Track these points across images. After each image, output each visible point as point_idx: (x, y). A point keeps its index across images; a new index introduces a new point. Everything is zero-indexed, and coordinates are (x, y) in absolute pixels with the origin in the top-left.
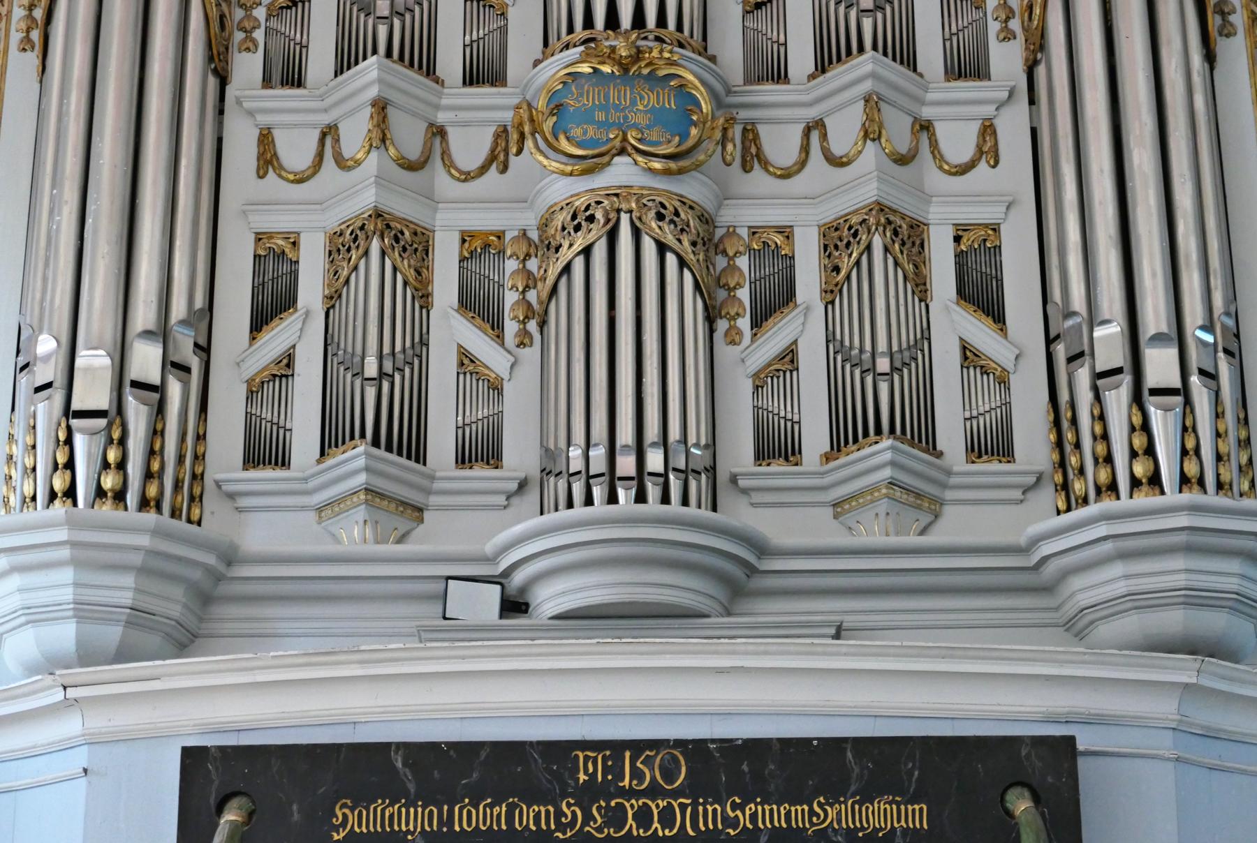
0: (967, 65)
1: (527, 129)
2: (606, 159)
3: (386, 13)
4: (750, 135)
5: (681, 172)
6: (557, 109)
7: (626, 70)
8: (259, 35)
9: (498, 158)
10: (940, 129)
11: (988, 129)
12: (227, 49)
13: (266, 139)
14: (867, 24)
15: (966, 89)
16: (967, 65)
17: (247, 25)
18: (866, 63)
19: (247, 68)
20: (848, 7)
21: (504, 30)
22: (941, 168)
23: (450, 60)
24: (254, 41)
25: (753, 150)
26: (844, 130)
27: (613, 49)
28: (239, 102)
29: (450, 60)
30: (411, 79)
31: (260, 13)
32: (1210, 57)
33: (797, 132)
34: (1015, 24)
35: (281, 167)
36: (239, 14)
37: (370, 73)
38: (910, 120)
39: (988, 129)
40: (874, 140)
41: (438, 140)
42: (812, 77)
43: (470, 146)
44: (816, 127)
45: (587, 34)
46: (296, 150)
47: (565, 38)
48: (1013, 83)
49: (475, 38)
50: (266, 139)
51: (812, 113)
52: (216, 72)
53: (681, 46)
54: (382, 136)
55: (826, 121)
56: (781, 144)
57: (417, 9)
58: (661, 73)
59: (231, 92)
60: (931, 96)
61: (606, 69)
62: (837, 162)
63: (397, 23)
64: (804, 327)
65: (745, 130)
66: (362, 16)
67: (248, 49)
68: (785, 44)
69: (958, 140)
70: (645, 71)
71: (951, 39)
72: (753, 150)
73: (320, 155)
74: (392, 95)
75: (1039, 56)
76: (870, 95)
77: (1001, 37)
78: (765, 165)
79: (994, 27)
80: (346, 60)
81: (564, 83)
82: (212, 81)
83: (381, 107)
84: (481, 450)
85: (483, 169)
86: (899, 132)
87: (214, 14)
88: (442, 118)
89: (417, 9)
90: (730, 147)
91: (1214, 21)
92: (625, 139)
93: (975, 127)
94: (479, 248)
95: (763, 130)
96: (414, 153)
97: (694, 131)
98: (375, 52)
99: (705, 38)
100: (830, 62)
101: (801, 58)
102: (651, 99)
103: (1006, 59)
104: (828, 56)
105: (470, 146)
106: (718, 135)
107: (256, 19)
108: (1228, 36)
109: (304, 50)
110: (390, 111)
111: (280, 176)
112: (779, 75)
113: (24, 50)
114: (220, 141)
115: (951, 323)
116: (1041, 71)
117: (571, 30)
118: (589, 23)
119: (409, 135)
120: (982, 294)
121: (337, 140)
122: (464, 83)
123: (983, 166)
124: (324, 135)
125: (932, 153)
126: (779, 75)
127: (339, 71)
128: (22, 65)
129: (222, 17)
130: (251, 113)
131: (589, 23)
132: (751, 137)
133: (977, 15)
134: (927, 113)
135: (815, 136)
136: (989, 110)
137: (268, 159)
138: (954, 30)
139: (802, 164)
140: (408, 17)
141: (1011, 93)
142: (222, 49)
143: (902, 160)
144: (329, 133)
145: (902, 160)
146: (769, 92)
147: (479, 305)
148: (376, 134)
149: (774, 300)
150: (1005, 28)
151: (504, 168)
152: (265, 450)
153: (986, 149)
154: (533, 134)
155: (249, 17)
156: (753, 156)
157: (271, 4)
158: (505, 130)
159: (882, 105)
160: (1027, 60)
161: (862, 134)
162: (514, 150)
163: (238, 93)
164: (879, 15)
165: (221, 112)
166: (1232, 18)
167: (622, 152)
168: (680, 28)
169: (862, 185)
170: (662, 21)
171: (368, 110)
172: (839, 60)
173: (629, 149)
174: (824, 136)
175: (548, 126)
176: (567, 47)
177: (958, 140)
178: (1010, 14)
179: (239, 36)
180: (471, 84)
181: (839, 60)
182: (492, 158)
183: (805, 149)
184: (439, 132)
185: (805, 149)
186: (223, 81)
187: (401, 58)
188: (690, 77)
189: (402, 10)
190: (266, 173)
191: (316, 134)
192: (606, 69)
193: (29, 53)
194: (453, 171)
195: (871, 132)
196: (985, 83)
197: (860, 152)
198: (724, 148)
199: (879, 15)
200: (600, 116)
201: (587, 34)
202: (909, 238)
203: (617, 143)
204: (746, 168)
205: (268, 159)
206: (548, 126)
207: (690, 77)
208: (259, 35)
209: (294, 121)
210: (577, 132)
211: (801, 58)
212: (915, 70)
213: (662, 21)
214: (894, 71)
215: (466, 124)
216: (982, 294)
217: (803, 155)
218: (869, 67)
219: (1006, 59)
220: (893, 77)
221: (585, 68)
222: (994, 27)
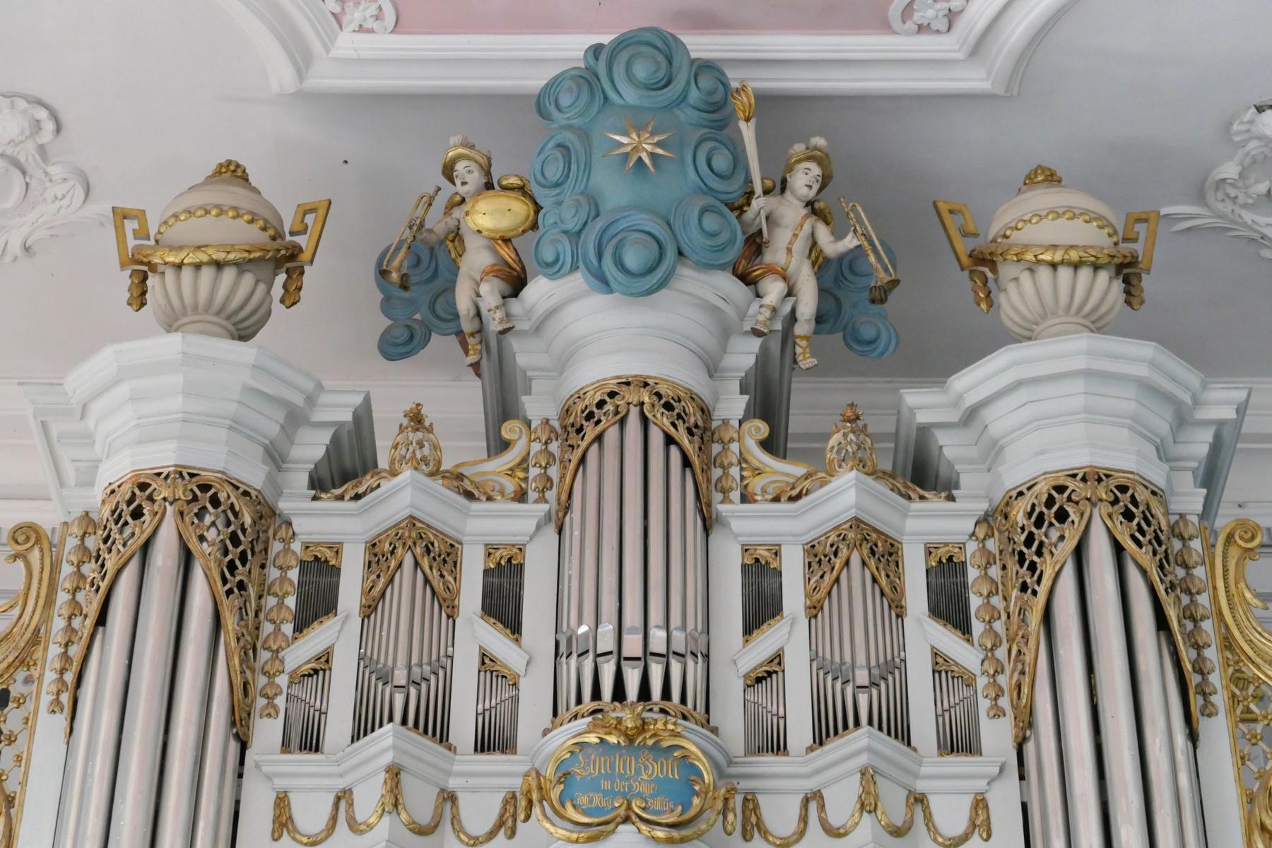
0: (958, 741)
1: (535, 796)
2: (611, 827)
3: (403, 682)
4: (751, 805)
5: (683, 840)
6: (565, 777)
7: (631, 740)
8: (280, 701)
9: (506, 823)
10: (935, 803)
11: (980, 804)
12: (249, 714)
13: (282, 802)
14: (863, 699)
15: (959, 764)
16: (958, 741)
17: (270, 692)
18: (862, 739)
19: (267, 732)
20: (846, 682)
21: (515, 700)
22: (935, 840)
23: (463, 727)
24: (275, 707)
25: (754, 820)
26: (842, 801)
27: (619, 720)
28: (258, 766)
29: (463, 727)
30: (425, 746)
31: (282, 681)
32: (1193, 737)
33: (795, 803)
34: (1004, 702)
35: (296, 830)
36: (262, 681)
37: (387, 740)
38: (904, 793)
39: (980, 804)
40: (870, 812)
41: (448, 805)
42: (810, 749)
43: (479, 812)
44: (814, 798)
45: (595, 705)
46: (311, 813)
47: (574, 708)
48: (1003, 759)
49: (487, 706)
50: (282, 802)
51: (810, 785)
52: (237, 736)
53: (685, 717)
54: (395, 800)
55: (824, 793)
57: (433, 678)
58: (665, 744)
59: (249, 754)
60: (924, 770)
61: (613, 739)
62: (834, 833)
63: (413, 691)
65: (745, 799)
66: (380, 684)
67: (269, 715)
68: (785, 717)
70: (650, 742)
71: (943, 716)
72: (754, 820)
73: (334, 819)
74: (405, 761)
75: (1028, 733)
76: (866, 769)
77: (992, 714)
78: (765, 834)
79: (984, 704)
80: (363, 727)
81: (572, 752)
82: (234, 746)
83: (395, 773)
85: (492, 835)
86: (894, 805)
87: (238, 682)
88: (453, 784)
89: (433, 678)
90: (731, 817)
91: (1196, 702)
92: (629, 808)
93: (966, 802)
95: (761, 799)
96: (425, 818)
97: (696, 801)
98: (391, 720)
99: (707, 711)
100: (828, 735)
101: (800, 729)
102: (655, 769)
103: (996, 735)
104: (824, 731)
106: (719, 805)
107: (278, 686)
108: (1209, 716)
109: (323, 717)
110: (403, 776)
111: (294, 839)
112: (777, 746)
113: (53, 712)
114: (238, 803)
116: (1030, 748)
117: (579, 701)
118: (596, 695)
119: (421, 802)
121: (351, 804)
122: (476, 750)
123: (976, 838)
124: (338, 799)
125: (927, 825)
126: (777, 746)
127: (355, 738)
128: (50, 726)
129: (246, 684)
130: (269, 777)
131: (596, 695)
132: (751, 806)
133: (967, 692)
134: (921, 786)
135: (813, 806)
136: (981, 785)
137: (283, 822)
138: (946, 706)
139: (801, 834)
140: (424, 685)
141: (1002, 769)
142: (244, 715)
143: (898, 832)
144: (343, 797)
145: (898, 832)
146: (769, 763)
148: (389, 800)
150: (995, 705)
151: (512, 834)
153: (978, 822)
154: (540, 802)
155: (271, 683)
157: (295, 671)
158: (514, 797)
159: (877, 778)
160: (1016, 737)
161: (858, 806)
162: (522, 816)
163: (257, 758)
164: (874, 692)
165: (240, 776)
166: (1213, 699)
167: (626, 820)
168: (683, 700)
170: (666, 694)
171: (382, 776)
172: (836, 733)
173: (633, 817)
174: (822, 807)
175: (555, 794)
176: (575, 717)
178: (999, 693)
179: (261, 702)
180: (482, 751)
181: (836, 733)
182: (500, 824)
183: (804, 819)
184: (450, 797)
185: (804, 819)
186: (244, 747)
187: (416, 725)
188: (693, 748)
189: (418, 679)
190: (281, 836)
191: (331, 798)
192: (613, 739)
193: (58, 715)
194: (462, 836)
195: (867, 805)
196: (977, 759)
197: (857, 824)
198: (725, 817)
199: (874, 692)
200: (606, 785)
201: (595, 705)
203: (622, 812)
204: (746, 836)
205: (283, 822)
206: (555, 794)
207: (693, 748)
208: (280, 701)
209: (310, 784)
210: (583, 800)
211: (800, 729)
212: (909, 744)
213: (666, 694)
214: (888, 746)
215: (475, 790)
217: (802, 826)
218: (865, 742)
219: (996, 735)
220: (887, 751)
221: (592, 738)
222: (984, 704)
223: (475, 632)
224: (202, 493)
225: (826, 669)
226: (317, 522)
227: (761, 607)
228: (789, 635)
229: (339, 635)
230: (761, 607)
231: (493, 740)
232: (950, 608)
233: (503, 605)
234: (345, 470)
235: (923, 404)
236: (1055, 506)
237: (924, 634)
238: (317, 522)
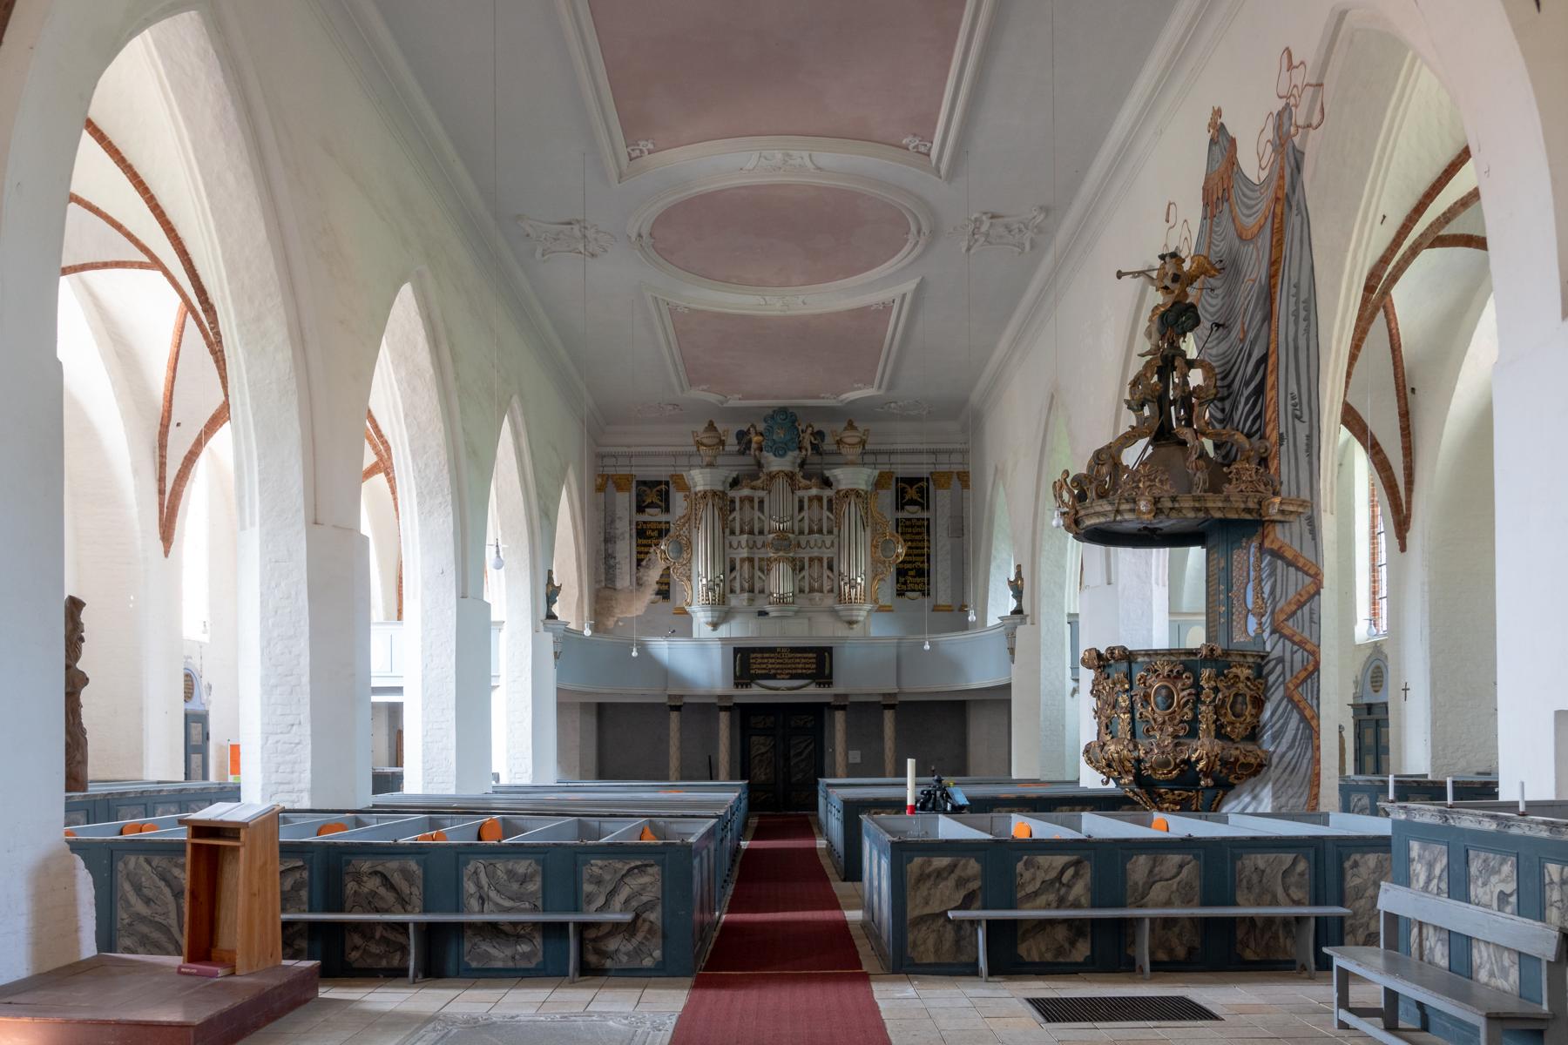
16: (830, 532)
43: (759, 544)
46: (735, 544)
56: (803, 544)
64: (805, 573)
69: (828, 543)
84: (762, 591)
94: (761, 560)
103: (835, 530)
105: (759, 544)
115: (826, 572)
120: (830, 568)
147: (761, 570)
149: (802, 569)
152: (732, 591)
156: (799, 545)
169: (816, 553)
177: (828, 543)
202: (820, 560)
209: (734, 540)
216: (830, 568)
223: (757, 514)
224: (714, 493)
225: (811, 520)
226: (731, 494)
227: (801, 509)
228: (805, 514)
229: (736, 514)
230: (801, 509)
231: (761, 532)
232: (830, 509)
233: (761, 509)
234: (735, 483)
235: (827, 473)
236: (847, 495)
237: (826, 513)
238: (731, 494)
